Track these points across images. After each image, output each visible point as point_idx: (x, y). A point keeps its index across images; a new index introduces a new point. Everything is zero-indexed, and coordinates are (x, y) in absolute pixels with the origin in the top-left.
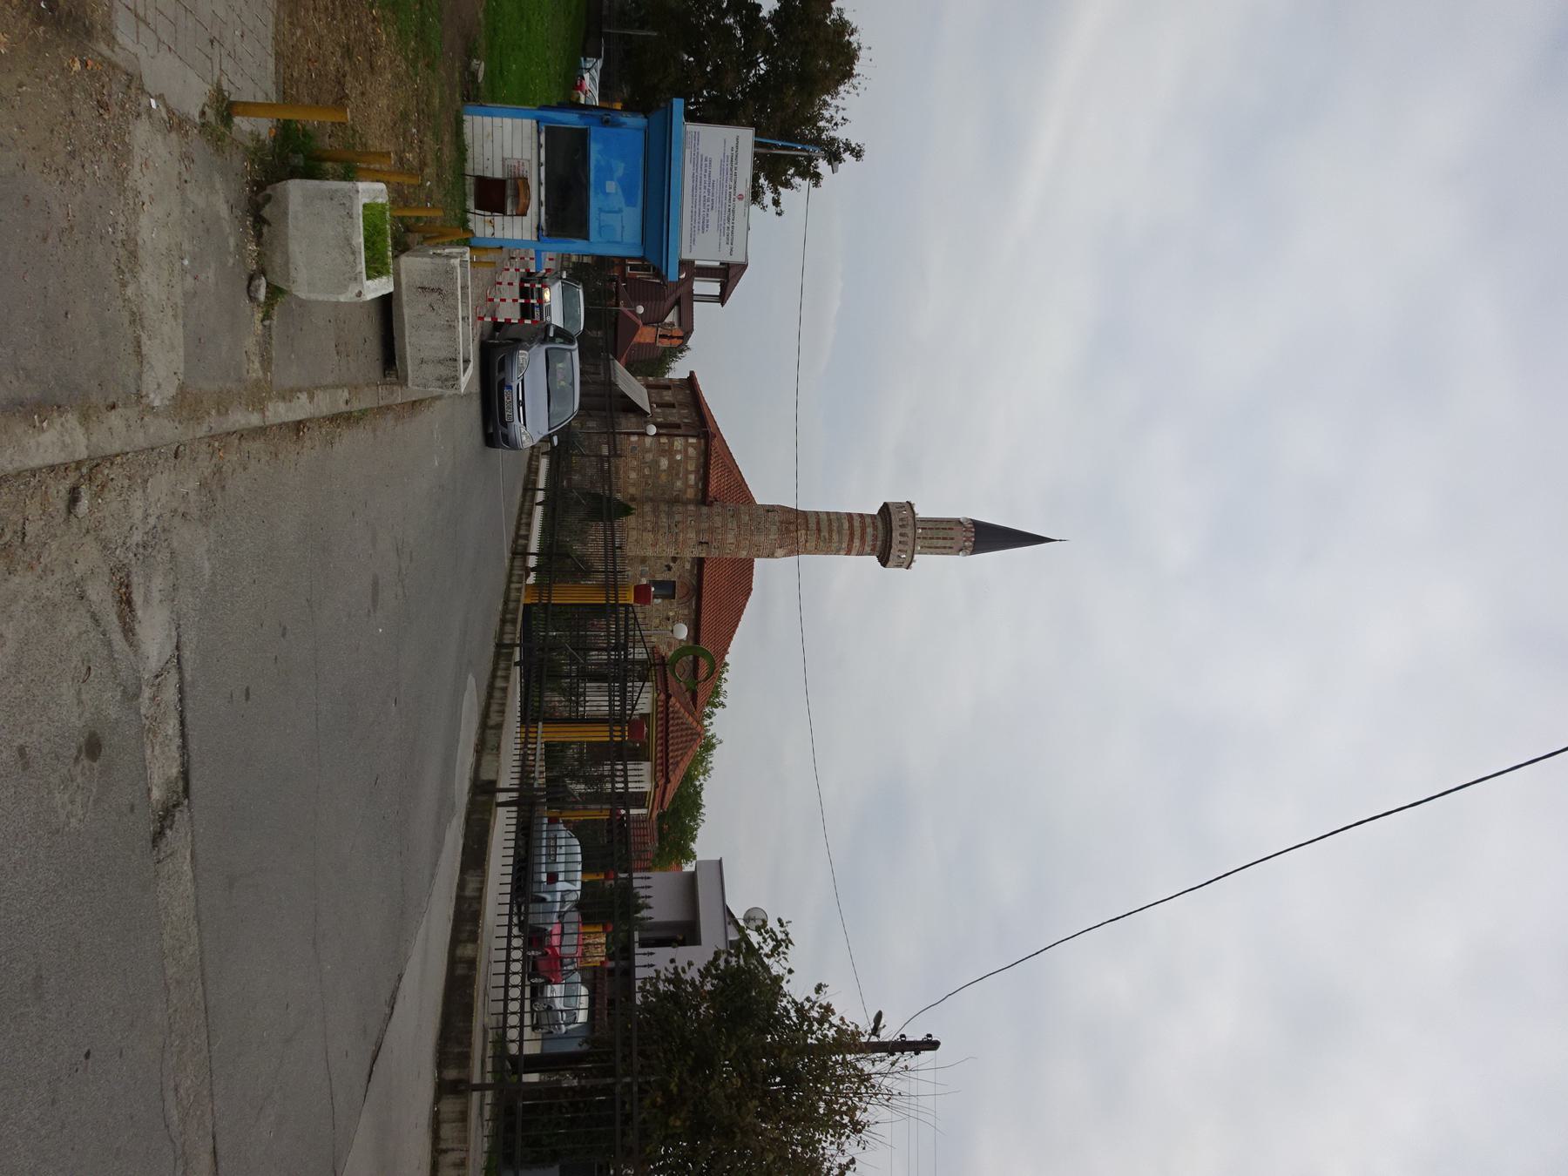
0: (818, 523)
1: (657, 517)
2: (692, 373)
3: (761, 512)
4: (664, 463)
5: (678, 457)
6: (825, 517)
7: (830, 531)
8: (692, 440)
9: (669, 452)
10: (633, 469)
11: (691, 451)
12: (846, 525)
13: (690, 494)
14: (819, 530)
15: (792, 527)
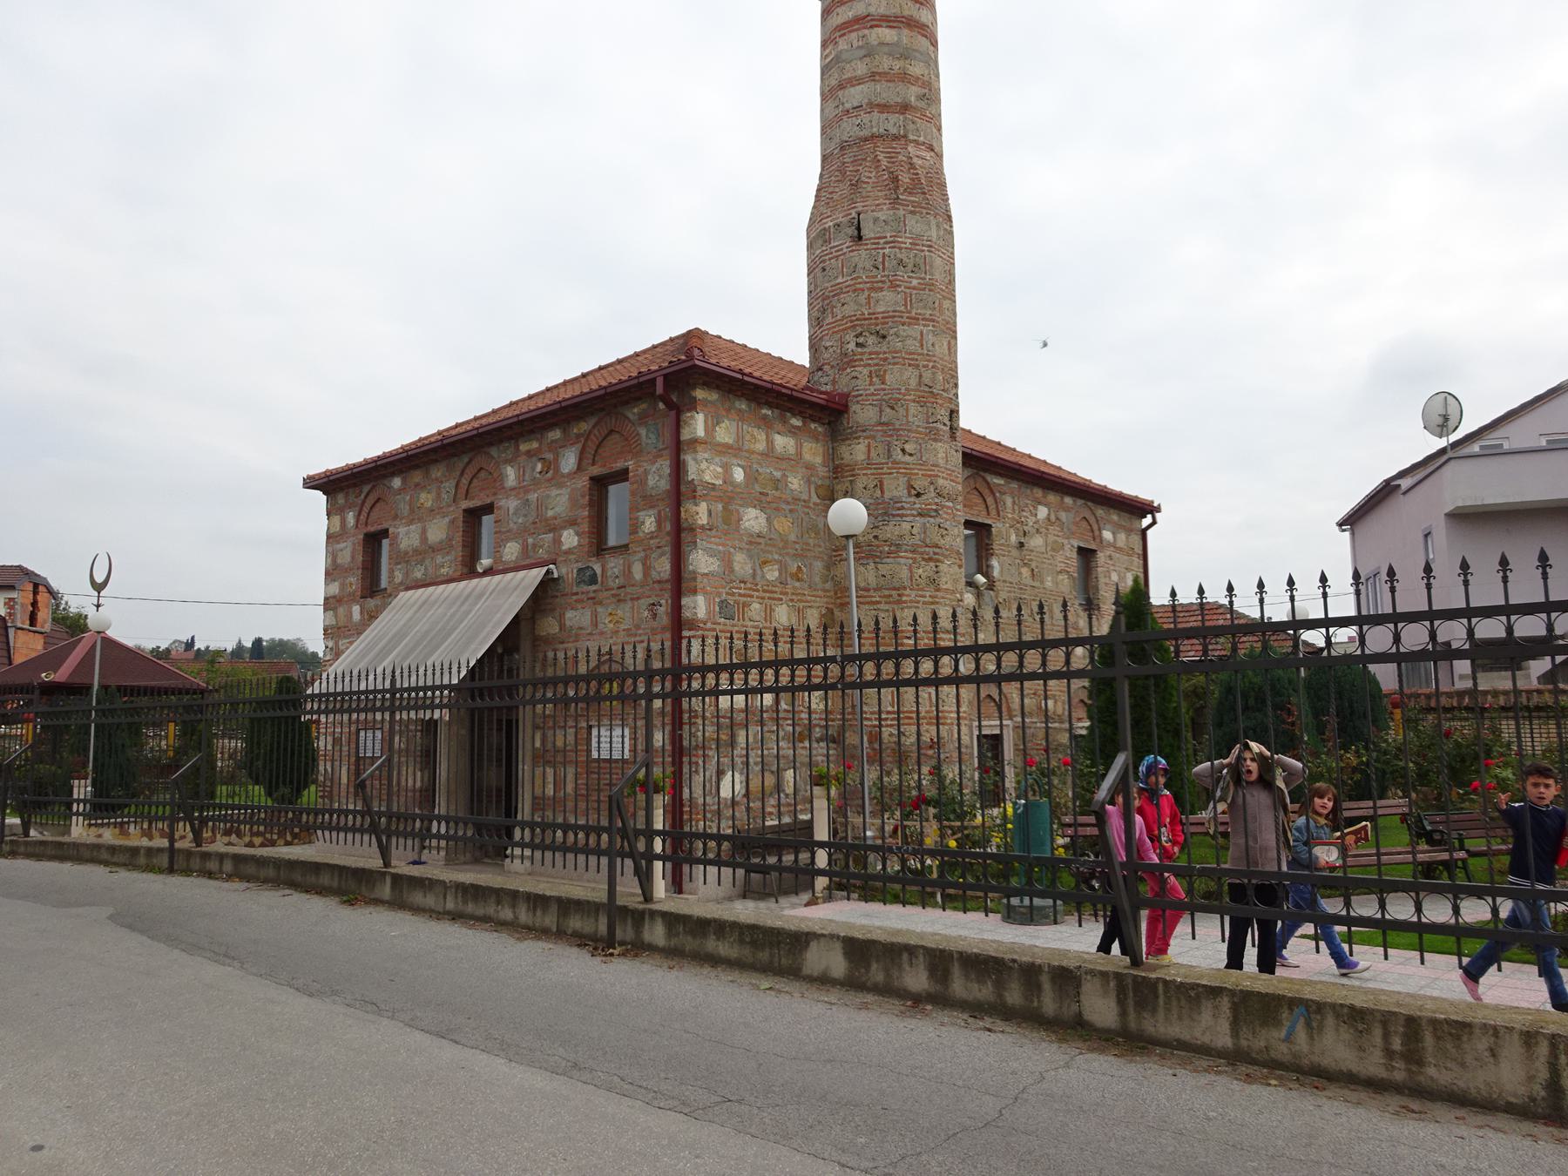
0: (884, 108)
1: (896, 547)
2: (312, 483)
3: (861, 257)
4: (753, 519)
5: (739, 475)
6: (831, 104)
7: (904, 77)
8: (697, 424)
9: (728, 497)
10: (769, 613)
11: (725, 433)
12: (886, 34)
13: (813, 453)
14: (905, 108)
15: (905, 178)
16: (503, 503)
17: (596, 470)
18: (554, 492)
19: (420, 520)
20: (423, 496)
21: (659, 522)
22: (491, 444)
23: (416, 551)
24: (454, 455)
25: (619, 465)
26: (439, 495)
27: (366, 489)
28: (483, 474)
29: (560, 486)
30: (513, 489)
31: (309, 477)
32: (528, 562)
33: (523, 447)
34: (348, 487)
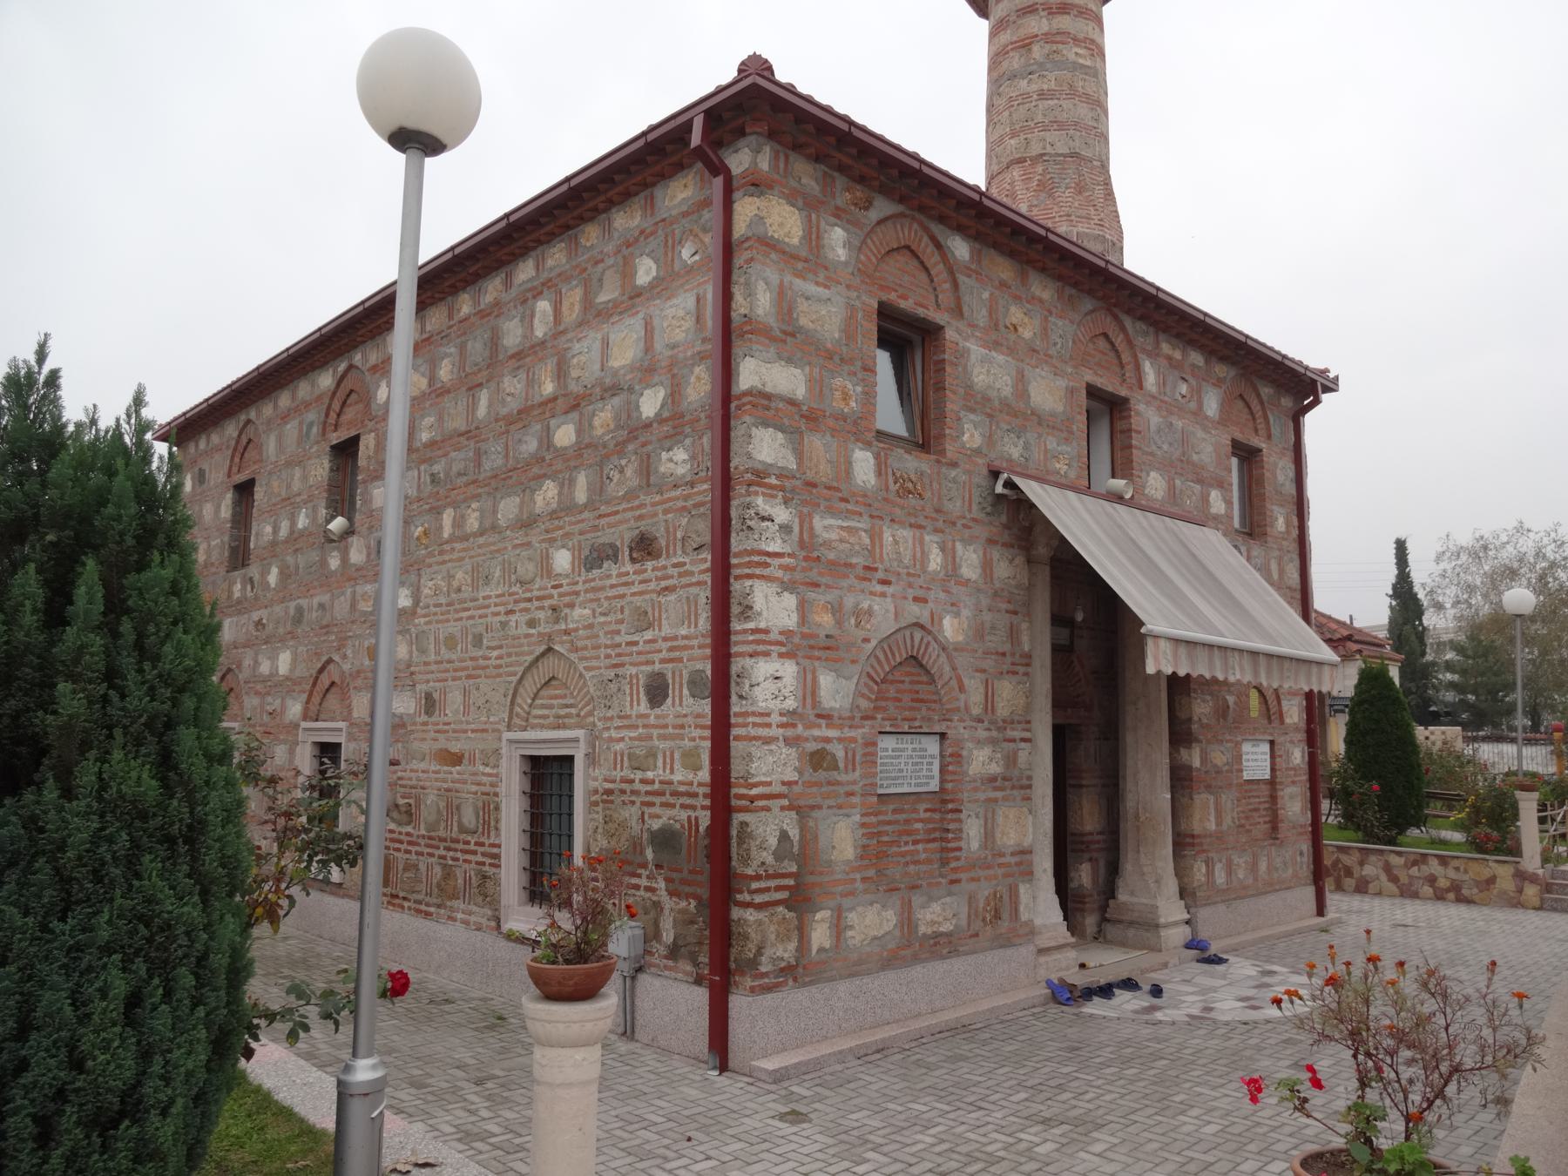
16: (1141, 407)
17: (1239, 436)
18: (1200, 434)
19: (1011, 351)
20: (1016, 314)
21: (1288, 523)
22: (1129, 312)
23: (1006, 406)
24: (1075, 285)
25: (1257, 442)
26: (1045, 332)
27: (883, 207)
28: (1102, 344)
29: (1205, 429)
30: (1154, 397)
31: (770, 69)
32: (1174, 510)
33: (1166, 348)
34: (841, 168)
